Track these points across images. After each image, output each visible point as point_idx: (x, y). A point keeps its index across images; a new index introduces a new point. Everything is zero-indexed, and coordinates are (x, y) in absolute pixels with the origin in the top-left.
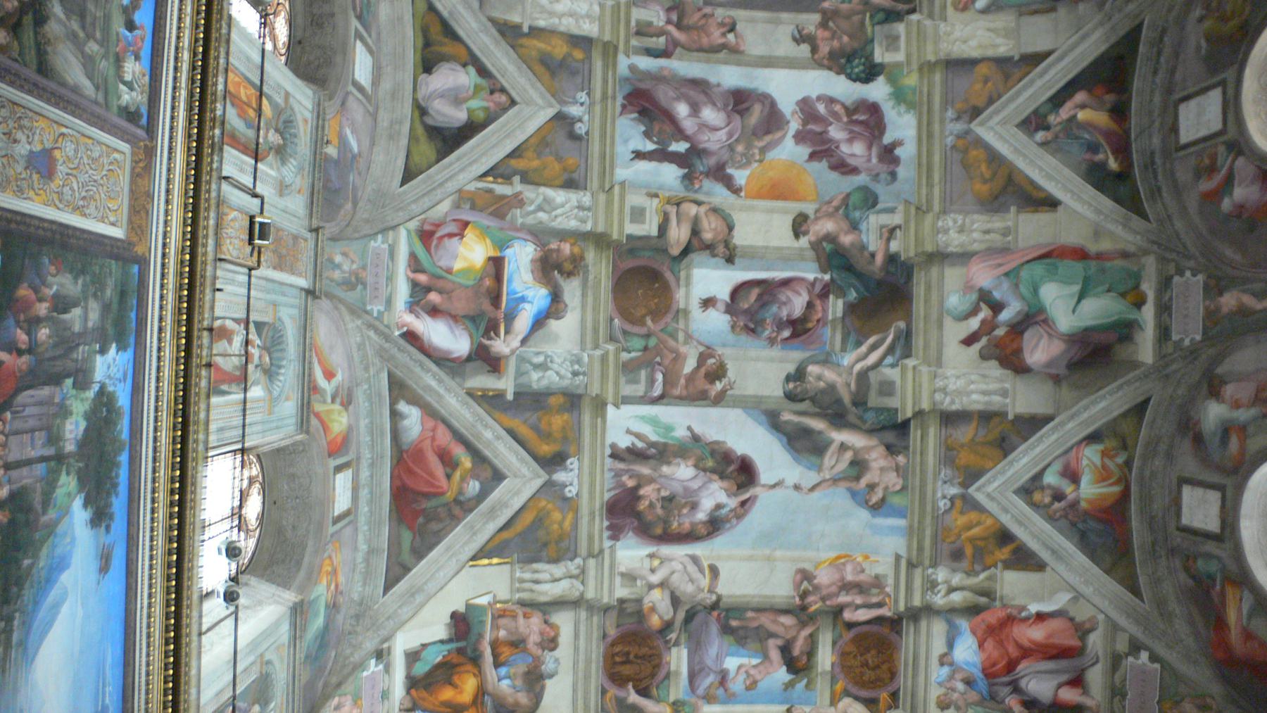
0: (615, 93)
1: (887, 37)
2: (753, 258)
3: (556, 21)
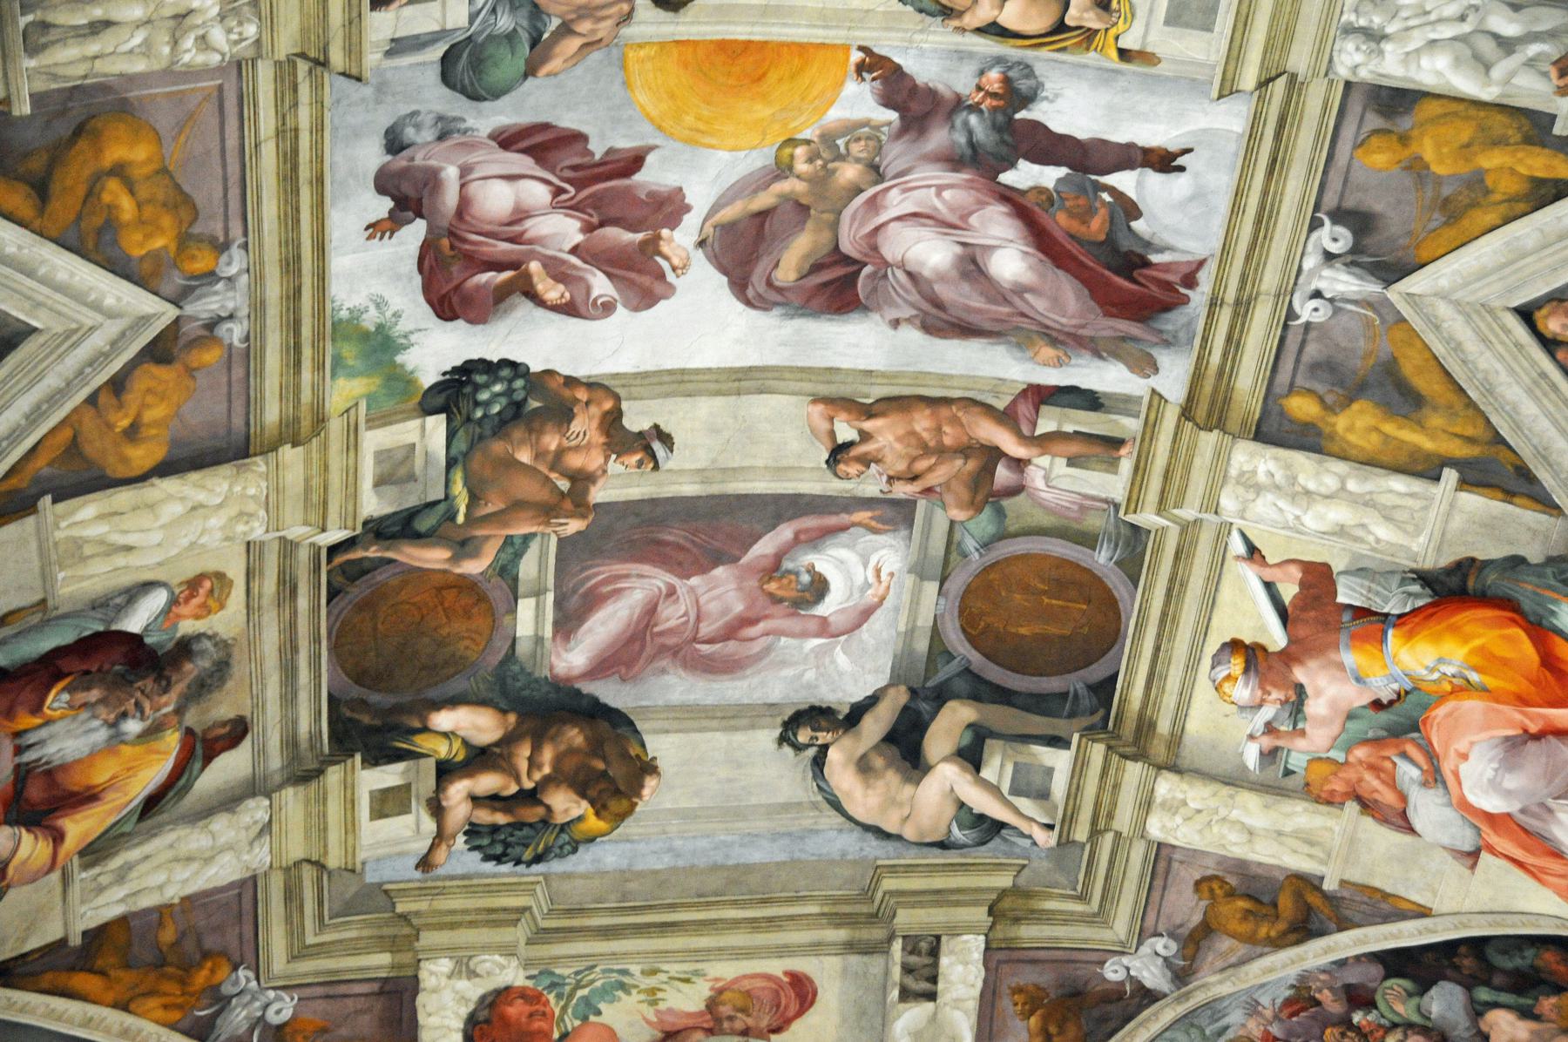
0: (1211, 315)
1: (411, 477)
3: (1352, 485)
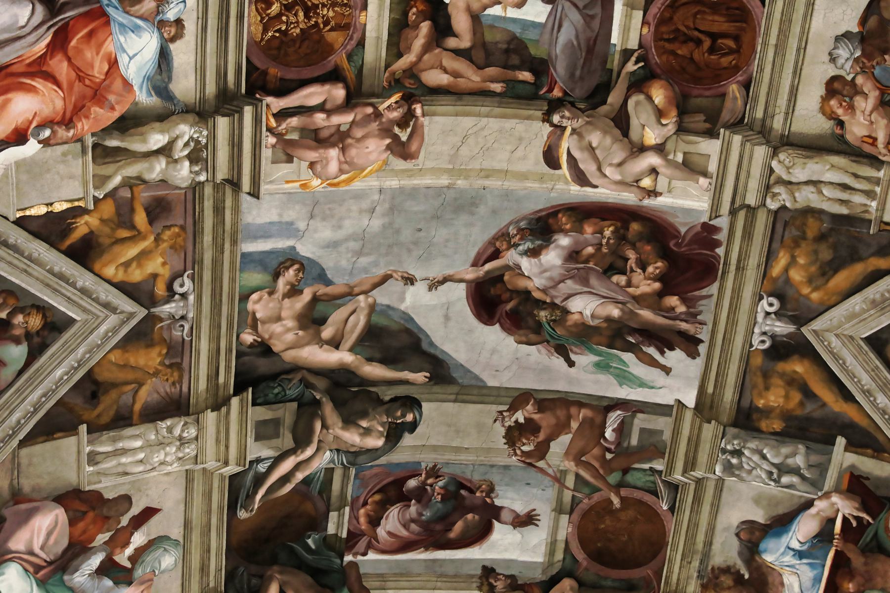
2: (455, 576)
